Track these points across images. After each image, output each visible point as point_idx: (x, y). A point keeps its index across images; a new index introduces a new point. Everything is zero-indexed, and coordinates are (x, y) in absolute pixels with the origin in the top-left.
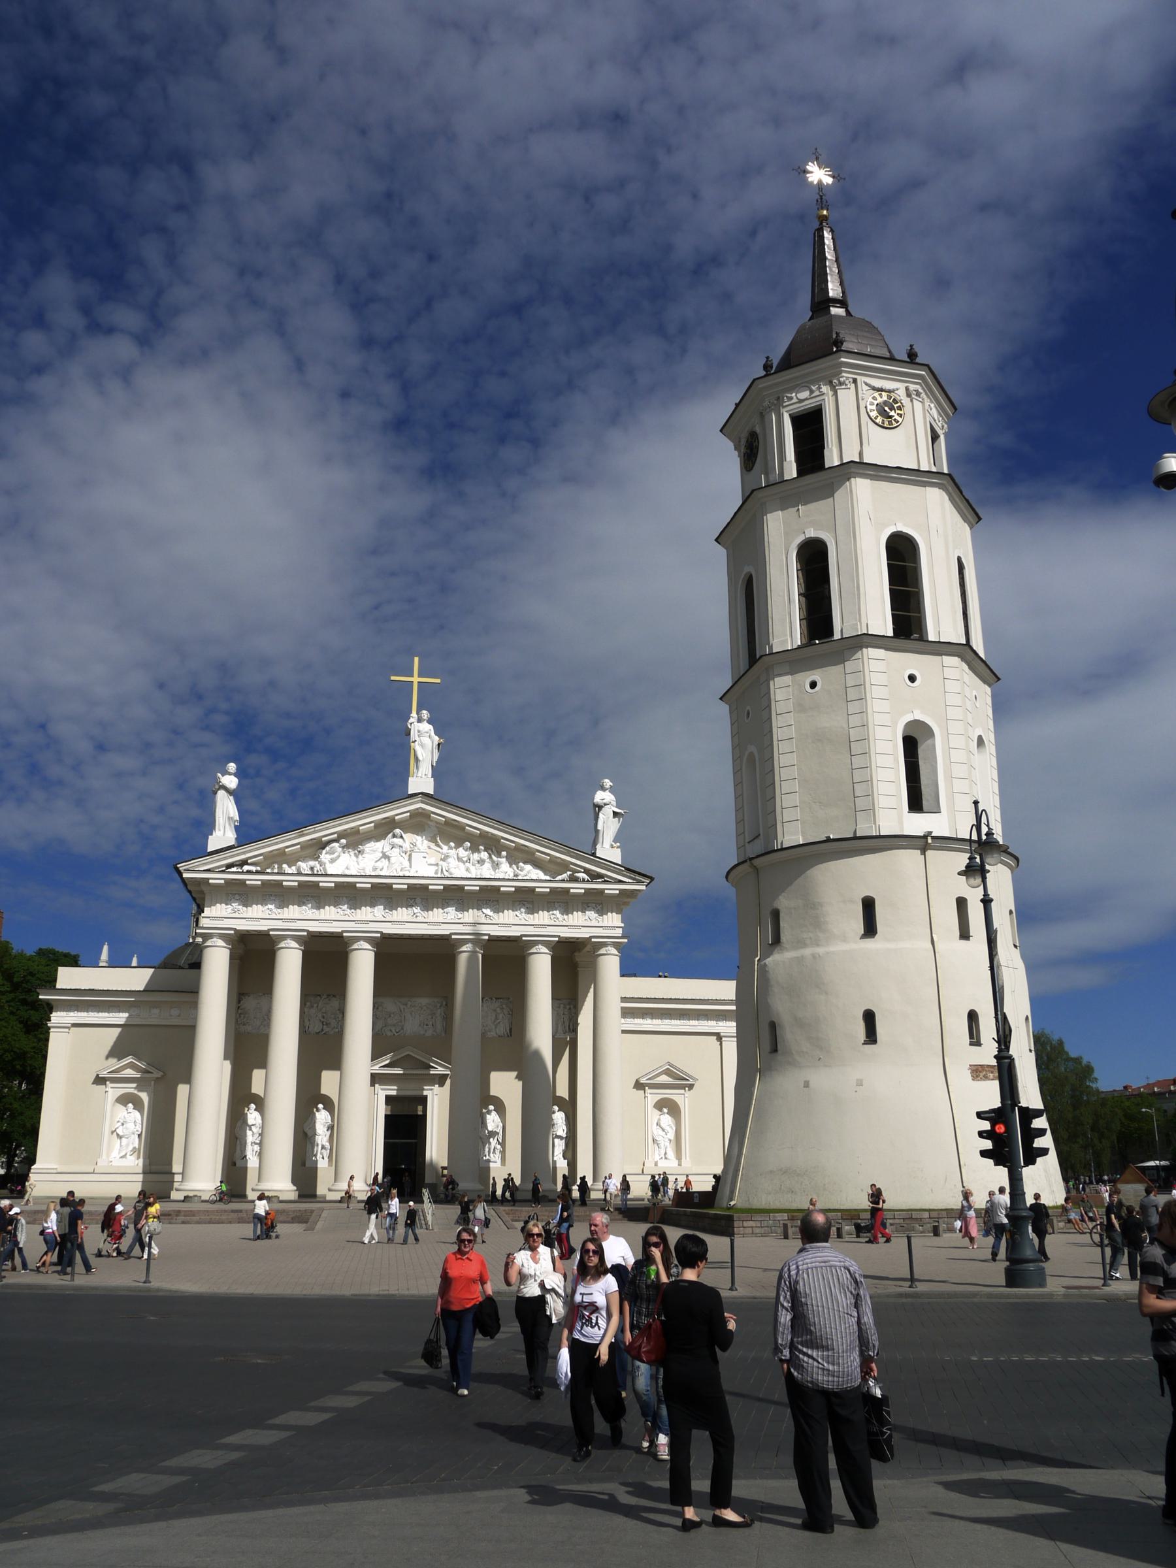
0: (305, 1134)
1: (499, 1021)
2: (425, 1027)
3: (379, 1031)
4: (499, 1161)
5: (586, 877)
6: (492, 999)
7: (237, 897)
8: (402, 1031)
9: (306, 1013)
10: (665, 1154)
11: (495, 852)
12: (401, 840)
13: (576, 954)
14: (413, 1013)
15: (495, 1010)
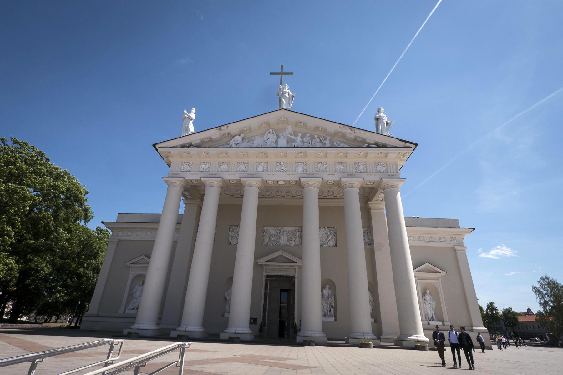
0: (225, 298)
1: (329, 239)
2: (290, 241)
3: (266, 244)
4: (334, 318)
5: (376, 147)
6: (325, 228)
7: (187, 164)
8: (278, 244)
9: (230, 234)
10: (432, 317)
11: (324, 139)
12: (273, 135)
13: (369, 203)
14: (284, 235)
15: (327, 234)
